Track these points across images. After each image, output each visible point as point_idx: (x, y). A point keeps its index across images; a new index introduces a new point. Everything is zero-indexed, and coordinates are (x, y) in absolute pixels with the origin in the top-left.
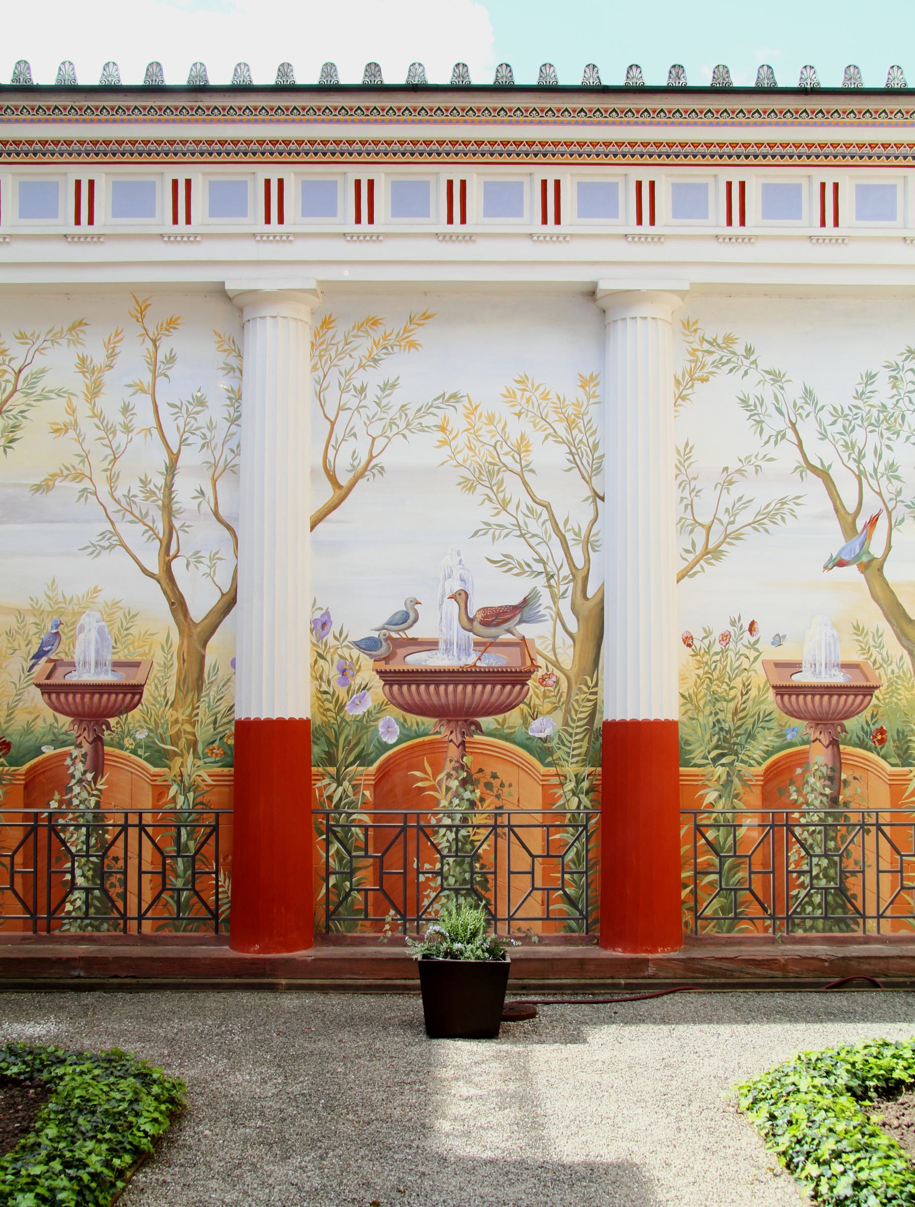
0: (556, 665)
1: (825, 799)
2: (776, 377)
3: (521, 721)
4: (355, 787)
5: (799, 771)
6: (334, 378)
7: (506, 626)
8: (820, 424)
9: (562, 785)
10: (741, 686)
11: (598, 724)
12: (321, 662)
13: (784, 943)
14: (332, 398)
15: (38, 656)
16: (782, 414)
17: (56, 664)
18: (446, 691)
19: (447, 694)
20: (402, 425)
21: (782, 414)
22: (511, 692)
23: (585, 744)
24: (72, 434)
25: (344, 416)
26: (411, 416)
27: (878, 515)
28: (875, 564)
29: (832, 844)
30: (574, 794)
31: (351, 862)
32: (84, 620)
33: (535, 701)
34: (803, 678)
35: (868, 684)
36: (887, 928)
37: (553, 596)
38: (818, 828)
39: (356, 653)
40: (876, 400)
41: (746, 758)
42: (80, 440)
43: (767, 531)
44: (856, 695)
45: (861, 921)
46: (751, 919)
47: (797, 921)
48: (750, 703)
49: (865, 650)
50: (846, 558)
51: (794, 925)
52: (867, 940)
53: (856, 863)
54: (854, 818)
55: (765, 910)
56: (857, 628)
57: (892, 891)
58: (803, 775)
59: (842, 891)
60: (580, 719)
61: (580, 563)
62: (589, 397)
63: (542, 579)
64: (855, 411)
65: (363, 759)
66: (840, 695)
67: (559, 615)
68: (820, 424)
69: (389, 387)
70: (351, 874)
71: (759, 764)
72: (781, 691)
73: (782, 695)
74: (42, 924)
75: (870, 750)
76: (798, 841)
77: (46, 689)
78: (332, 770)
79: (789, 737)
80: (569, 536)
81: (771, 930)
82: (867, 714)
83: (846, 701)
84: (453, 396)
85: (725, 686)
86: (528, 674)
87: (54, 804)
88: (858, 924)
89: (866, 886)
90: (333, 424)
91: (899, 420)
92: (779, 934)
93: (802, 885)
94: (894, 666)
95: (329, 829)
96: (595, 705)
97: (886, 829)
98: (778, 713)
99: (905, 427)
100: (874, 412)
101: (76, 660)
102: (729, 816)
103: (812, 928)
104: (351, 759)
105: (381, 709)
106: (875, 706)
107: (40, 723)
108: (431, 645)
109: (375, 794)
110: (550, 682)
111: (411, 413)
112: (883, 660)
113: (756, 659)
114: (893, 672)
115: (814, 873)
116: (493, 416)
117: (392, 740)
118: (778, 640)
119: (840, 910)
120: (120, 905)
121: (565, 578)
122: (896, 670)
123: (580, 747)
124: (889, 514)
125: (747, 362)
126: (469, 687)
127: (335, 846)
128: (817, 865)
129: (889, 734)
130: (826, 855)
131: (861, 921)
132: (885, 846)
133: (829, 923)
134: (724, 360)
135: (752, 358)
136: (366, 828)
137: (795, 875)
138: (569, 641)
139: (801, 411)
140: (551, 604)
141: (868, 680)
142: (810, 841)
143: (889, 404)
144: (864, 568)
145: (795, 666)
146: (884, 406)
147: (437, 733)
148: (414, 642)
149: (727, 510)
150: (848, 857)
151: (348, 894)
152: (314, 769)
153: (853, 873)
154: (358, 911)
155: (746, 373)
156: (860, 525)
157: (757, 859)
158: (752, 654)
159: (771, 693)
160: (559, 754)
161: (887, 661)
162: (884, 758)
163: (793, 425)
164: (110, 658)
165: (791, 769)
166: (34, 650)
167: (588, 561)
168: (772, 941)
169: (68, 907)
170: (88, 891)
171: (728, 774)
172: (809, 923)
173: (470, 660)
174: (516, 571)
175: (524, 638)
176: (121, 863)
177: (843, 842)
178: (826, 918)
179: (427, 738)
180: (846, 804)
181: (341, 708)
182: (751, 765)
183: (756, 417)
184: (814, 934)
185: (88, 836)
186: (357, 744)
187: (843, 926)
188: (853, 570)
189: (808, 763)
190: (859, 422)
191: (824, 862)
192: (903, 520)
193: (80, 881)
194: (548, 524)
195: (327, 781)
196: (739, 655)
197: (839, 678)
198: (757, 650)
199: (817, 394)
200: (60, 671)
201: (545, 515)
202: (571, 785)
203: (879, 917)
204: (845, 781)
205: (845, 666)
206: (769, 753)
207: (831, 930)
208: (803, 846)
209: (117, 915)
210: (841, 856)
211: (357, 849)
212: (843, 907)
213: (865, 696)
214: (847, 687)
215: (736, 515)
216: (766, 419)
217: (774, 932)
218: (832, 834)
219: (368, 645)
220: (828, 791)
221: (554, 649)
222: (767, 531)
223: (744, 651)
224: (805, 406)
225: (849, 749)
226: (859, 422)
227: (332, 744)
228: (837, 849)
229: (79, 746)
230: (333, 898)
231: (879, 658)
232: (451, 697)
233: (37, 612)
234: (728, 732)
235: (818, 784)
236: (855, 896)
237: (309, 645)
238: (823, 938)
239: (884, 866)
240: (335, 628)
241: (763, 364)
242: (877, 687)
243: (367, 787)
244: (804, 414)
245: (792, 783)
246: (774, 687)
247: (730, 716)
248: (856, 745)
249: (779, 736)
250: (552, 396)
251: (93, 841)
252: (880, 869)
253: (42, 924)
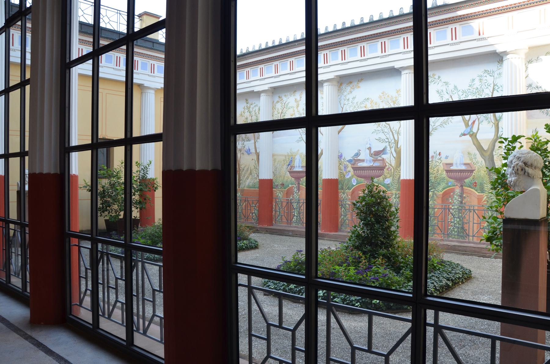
0: (391, 165)
1: (459, 202)
2: (446, 83)
3: (382, 180)
4: (347, 195)
5: (452, 194)
6: (343, 97)
7: (379, 155)
8: (459, 95)
9: (392, 196)
10: (436, 170)
12: (340, 165)
13: (446, 241)
14: (342, 102)
15: (288, 165)
16: (448, 94)
17: (292, 167)
18: (368, 172)
19: (366, 173)
21: (448, 94)
22: (380, 172)
23: (397, 185)
25: (345, 106)
26: (359, 105)
27: (475, 120)
28: (475, 134)
29: (460, 215)
30: (395, 198)
31: (346, 213)
32: (296, 157)
33: (386, 174)
34: (453, 168)
35: (472, 169)
36: (475, 240)
37: (390, 147)
38: (457, 210)
39: (347, 163)
40: (475, 87)
41: (437, 190)
43: (444, 127)
44: (468, 173)
45: (468, 237)
46: (438, 234)
47: (450, 235)
48: (439, 174)
49: (471, 159)
50: (466, 133)
51: (449, 236)
52: (469, 243)
53: (467, 220)
54: (467, 208)
55: (442, 232)
56: (469, 153)
57: (477, 229)
58: (453, 195)
59: (463, 228)
60: (396, 179)
61: (396, 139)
62: (399, 95)
63: (388, 143)
64: (469, 90)
65: (349, 188)
66: (464, 173)
67: (391, 152)
68: (459, 95)
69: (354, 98)
70: (345, 216)
71: (441, 192)
72: (447, 171)
73: (448, 173)
74: (289, 223)
75: (472, 188)
76: (451, 213)
77: (290, 172)
78: (343, 191)
79: (449, 184)
80: (394, 132)
81: (443, 237)
82: (471, 178)
83: (465, 174)
84: (368, 99)
85: (432, 170)
86: (384, 167)
87: (291, 197)
88: (467, 238)
89: (470, 227)
90: (343, 108)
91: (482, 91)
92: (445, 239)
93: (452, 226)
94: (479, 164)
95: (342, 205)
96: (400, 175)
97: (476, 211)
98: (446, 178)
99: (484, 93)
100: (474, 90)
101: (295, 165)
102: (433, 205)
103: (454, 238)
104: (346, 188)
105: (352, 176)
106: (474, 176)
107: (289, 179)
108: (363, 161)
109: (351, 197)
110: (389, 170)
111: (359, 104)
112: (476, 162)
113: (441, 162)
114: (479, 166)
115: (455, 222)
116: (376, 103)
117: (355, 184)
118: (447, 157)
119: (462, 233)
120: (302, 220)
121: (393, 143)
122: (480, 165)
123: (396, 186)
124: (479, 119)
125: (438, 80)
126: (371, 171)
127: (343, 209)
128: (456, 220)
129: (478, 184)
130: (459, 218)
131: (468, 237)
132: (476, 216)
133: (459, 237)
134: (433, 81)
135: (440, 79)
136: (349, 205)
137: (450, 223)
138: (394, 159)
139: (453, 92)
140: (390, 149)
141: (472, 168)
142: (454, 213)
143: (479, 87)
144: (471, 136)
145: (451, 164)
146: (477, 88)
147: (364, 182)
148: (359, 160)
149: (433, 122)
150: (465, 218)
151: (345, 221)
152: (339, 191)
153: (466, 223)
154: (347, 225)
155: (438, 83)
156: (470, 123)
157: (440, 218)
158: (440, 161)
159: (445, 172)
160: (391, 188)
161: (478, 162)
162: (476, 191)
163: (451, 96)
164: (301, 165)
165: (450, 193)
166: (288, 164)
167: (398, 138)
168: (443, 240)
169: (294, 220)
170: (297, 216)
171: (433, 194)
172: (453, 236)
173: (371, 164)
174: (382, 141)
175: (383, 159)
176: (303, 211)
177: (464, 214)
178: (458, 235)
179: (362, 184)
180: (465, 204)
181: (344, 176)
182: (439, 192)
183: (441, 96)
184: (454, 239)
185: (297, 204)
186: (348, 184)
187: (463, 238)
188: (468, 137)
189: (454, 191)
190: (470, 93)
191: (458, 220)
192: (483, 121)
193: (296, 214)
195: (341, 194)
196: (436, 162)
197: (463, 168)
198: (441, 160)
199: (458, 86)
200: (292, 168)
201: (388, 127)
203: (473, 236)
204: (464, 197)
205: (465, 164)
206: (444, 189)
207: (459, 239)
208: (452, 215)
209: (301, 222)
210: (463, 218)
211: (347, 210)
212: (463, 232)
213: (471, 173)
214: (466, 170)
215: (435, 123)
216: (444, 96)
217: (444, 238)
218: (461, 212)
219: (350, 161)
220: (460, 200)
221: (390, 161)
222: (444, 127)
223: (438, 161)
224: (455, 91)
225: (466, 188)
226: (470, 93)
228: (462, 216)
229: (296, 185)
230: (342, 221)
231: (475, 162)
232: (367, 173)
233: (288, 156)
234: (433, 183)
235: (457, 198)
236: (466, 230)
237: (337, 162)
238: (457, 241)
239: (475, 222)
240: (343, 157)
241: (443, 80)
242: (474, 170)
243: (350, 195)
244: (454, 93)
245: (450, 197)
246: (446, 170)
247: (433, 178)
248: (468, 187)
249: (446, 184)
250: (390, 96)
251: (298, 206)
252: (474, 222)
253: (289, 223)
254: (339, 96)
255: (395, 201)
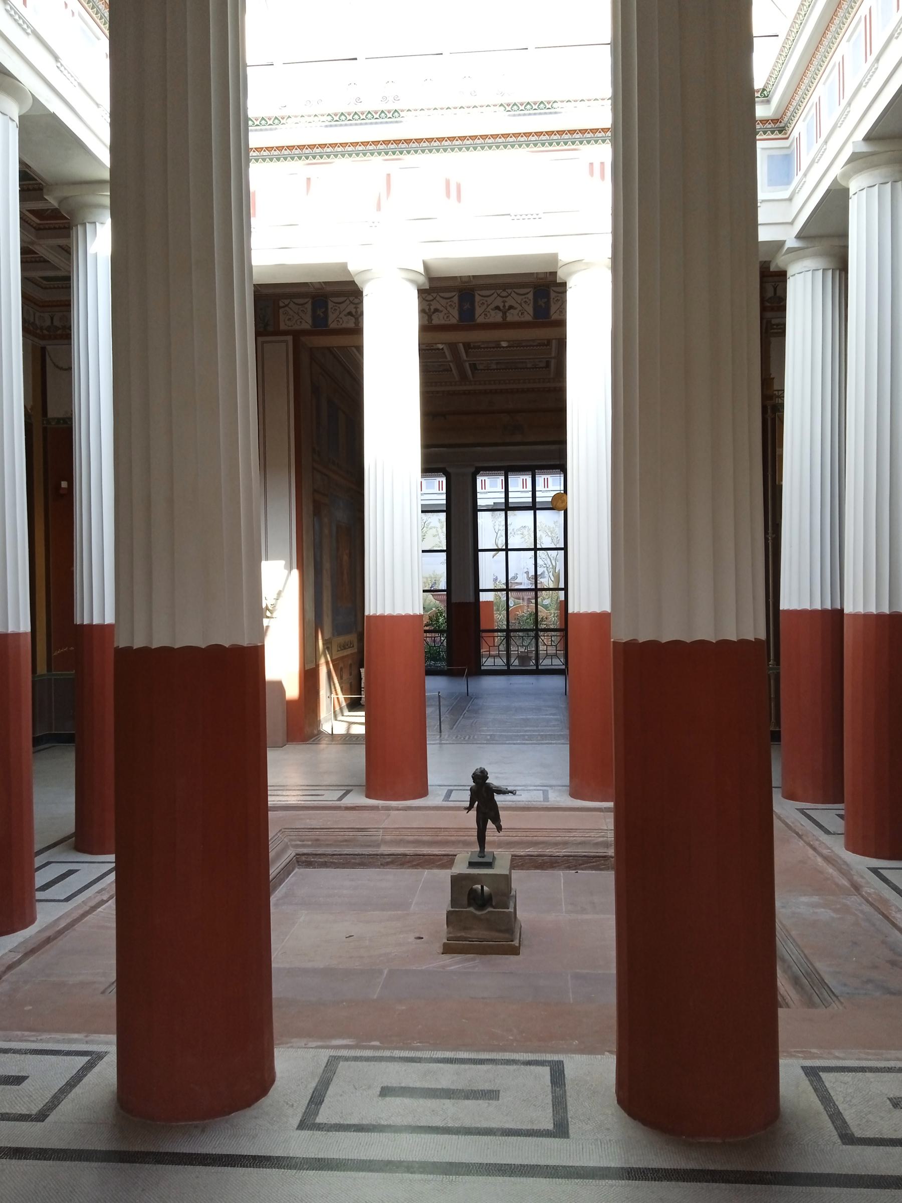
9: (551, 615)
11: (558, 601)
20: (513, 533)
24: (437, 537)
32: (441, 579)
33: (544, 596)
42: (439, 538)
61: (554, 564)
78: (499, 612)
80: (552, 558)
84: (525, 527)
107: (432, 603)
108: (521, 584)
111: (515, 530)
138: (552, 582)
166: (431, 586)
167: (556, 564)
194: (547, 556)
202: (553, 615)
227: (498, 607)
233: (431, 577)
254: (493, 521)
255: (553, 620)
